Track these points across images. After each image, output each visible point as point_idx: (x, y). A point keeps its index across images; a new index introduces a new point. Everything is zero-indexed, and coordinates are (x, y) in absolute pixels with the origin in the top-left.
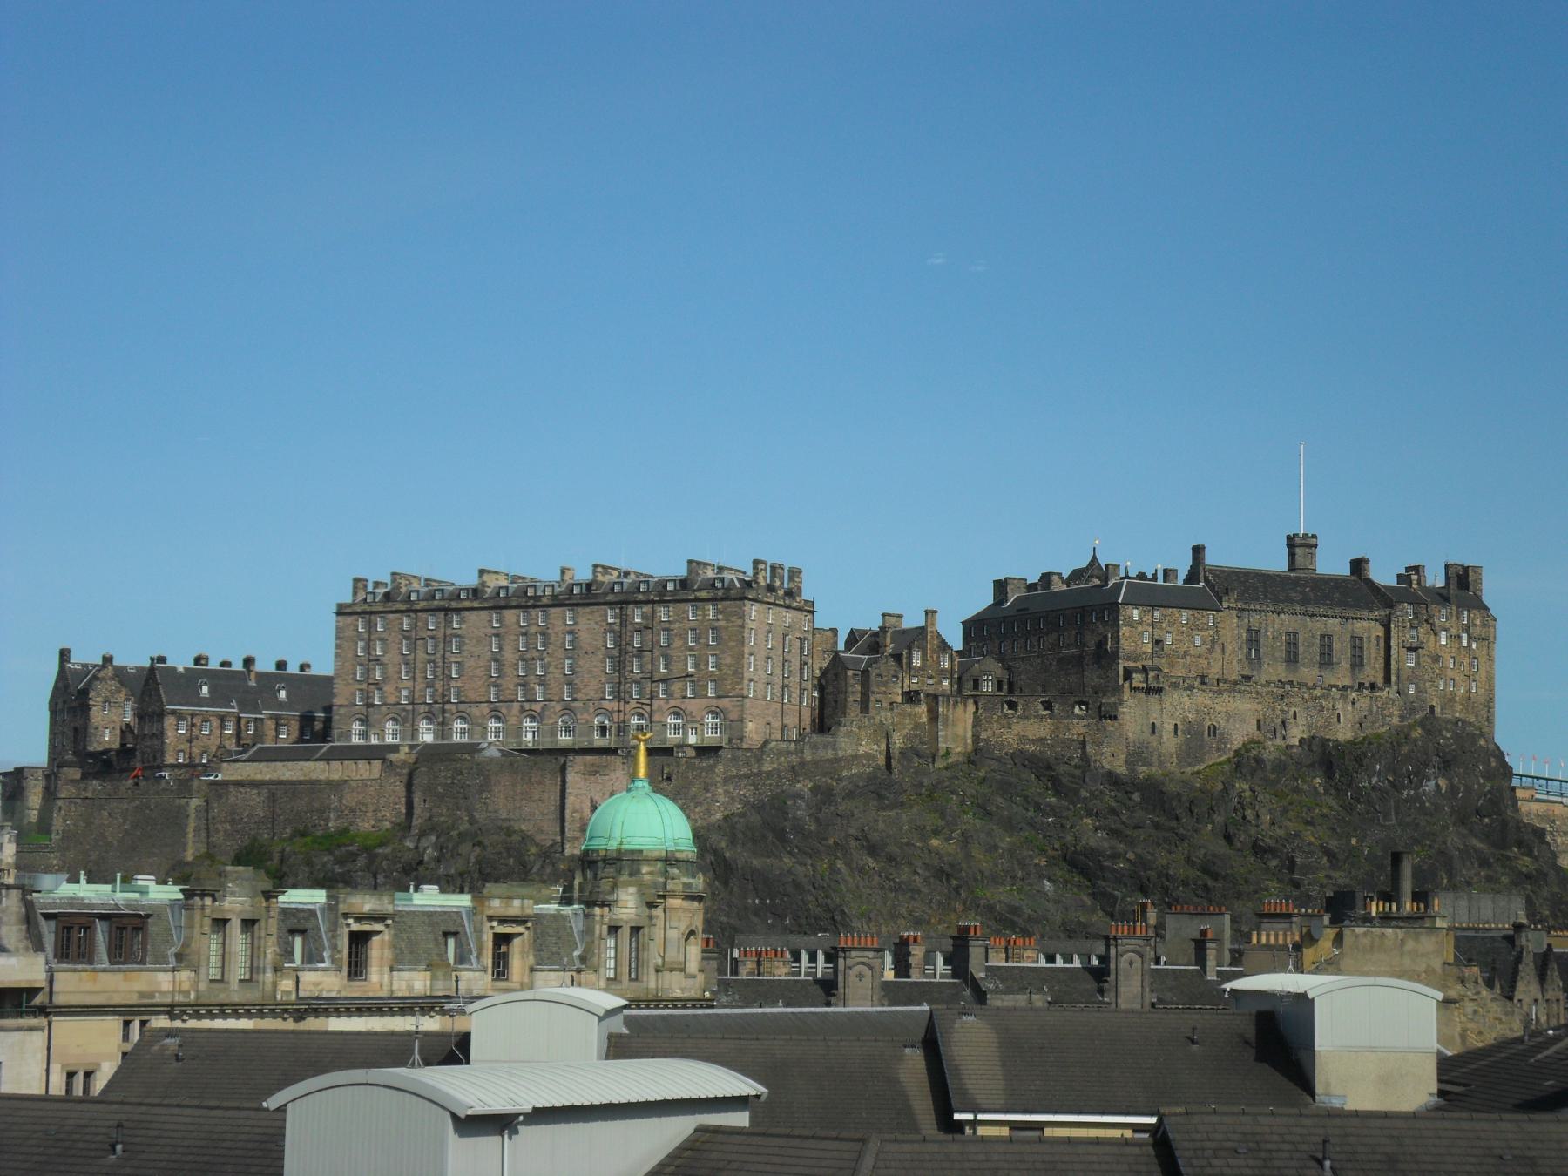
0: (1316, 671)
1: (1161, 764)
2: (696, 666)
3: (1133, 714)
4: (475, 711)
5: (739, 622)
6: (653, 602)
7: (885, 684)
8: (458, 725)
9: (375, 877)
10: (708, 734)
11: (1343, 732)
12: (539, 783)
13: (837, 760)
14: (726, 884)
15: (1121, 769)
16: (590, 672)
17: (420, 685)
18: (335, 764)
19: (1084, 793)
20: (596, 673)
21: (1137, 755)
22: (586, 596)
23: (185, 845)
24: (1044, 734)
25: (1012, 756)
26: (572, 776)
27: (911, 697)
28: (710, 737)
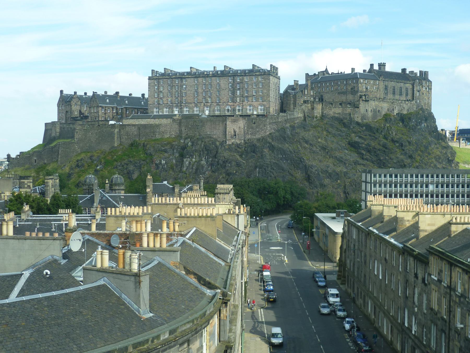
0: (399, 97)
1: (368, 120)
2: (256, 93)
3: (363, 106)
4: (191, 105)
7: (299, 99)
8: (185, 109)
9: (173, 150)
10: (259, 111)
11: (405, 112)
13: (294, 118)
14: (273, 152)
15: (360, 121)
16: (224, 95)
17: (174, 98)
18: (157, 120)
19: (352, 127)
20: (226, 95)
21: (363, 117)
22: (216, 74)
24: (340, 112)
27: (305, 102)
28: (260, 112)
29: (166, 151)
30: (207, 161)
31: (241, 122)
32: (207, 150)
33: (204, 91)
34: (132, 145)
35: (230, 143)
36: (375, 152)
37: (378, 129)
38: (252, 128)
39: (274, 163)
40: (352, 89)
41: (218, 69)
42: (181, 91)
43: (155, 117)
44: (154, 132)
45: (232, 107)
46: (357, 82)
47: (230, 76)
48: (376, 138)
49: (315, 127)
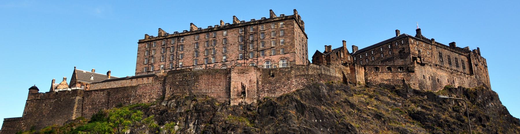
5: (292, 27)
13: (331, 76)
15: (418, 89)
16: (232, 51)
17: (168, 63)
19: (408, 96)
23: (73, 113)
24: (389, 78)
30: (197, 128)
31: (253, 73)
33: (206, 50)
35: (237, 104)
36: (449, 126)
38: (270, 83)
39: (305, 130)
40: (400, 52)
42: (177, 52)
48: (445, 110)
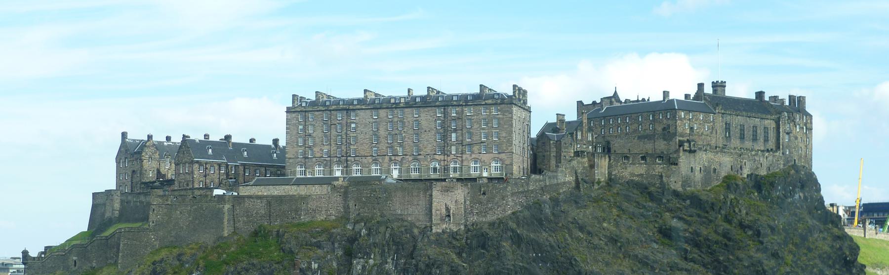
0: (751, 143)
1: (695, 186)
3: (684, 161)
6: (462, 105)
7: (567, 148)
8: (354, 168)
9: (333, 244)
10: (493, 172)
11: (763, 172)
12: (418, 196)
13: (558, 184)
14: (519, 247)
15: (680, 189)
17: (334, 148)
18: (302, 187)
19: (664, 201)
20: (430, 141)
21: (686, 182)
22: (412, 103)
24: (643, 172)
25: (627, 183)
26: (435, 193)
27: (577, 154)
28: (495, 173)
29: (319, 246)
31: (460, 191)
32: (396, 244)
33: (389, 134)
34: (256, 234)
35: (440, 231)
36: (709, 247)
37: (713, 204)
38: (481, 203)
39: (521, 268)
40: (664, 129)
41: (416, 93)
43: (299, 182)
44: (297, 211)
45: (442, 163)
46: (674, 117)
47: (438, 106)
48: (711, 221)
49: (596, 200)
